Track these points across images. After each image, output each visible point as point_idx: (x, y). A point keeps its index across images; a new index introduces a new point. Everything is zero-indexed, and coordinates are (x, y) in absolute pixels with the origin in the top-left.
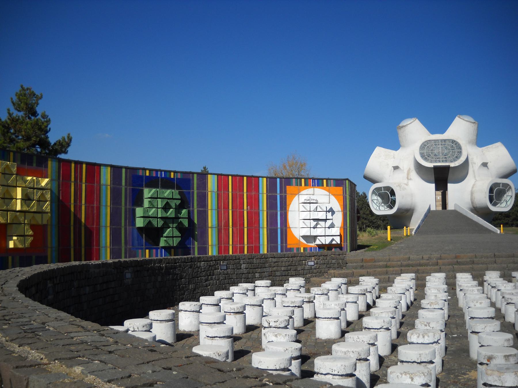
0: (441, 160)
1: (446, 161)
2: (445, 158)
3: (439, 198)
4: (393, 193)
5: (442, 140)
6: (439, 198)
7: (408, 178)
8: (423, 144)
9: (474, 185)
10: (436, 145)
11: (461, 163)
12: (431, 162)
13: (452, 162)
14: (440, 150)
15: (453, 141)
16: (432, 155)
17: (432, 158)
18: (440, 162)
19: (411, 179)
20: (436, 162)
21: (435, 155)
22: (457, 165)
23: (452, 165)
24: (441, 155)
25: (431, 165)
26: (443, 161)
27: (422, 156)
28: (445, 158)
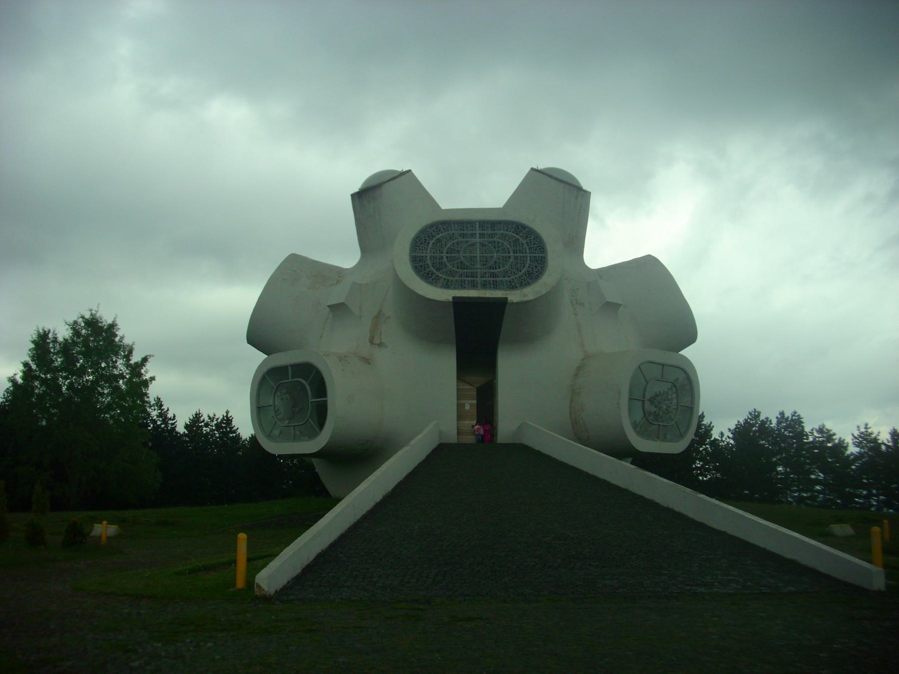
0: (479, 280)
1: (495, 286)
2: (493, 275)
3: (470, 405)
4: (320, 387)
5: (483, 224)
6: (467, 407)
7: (371, 342)
8: (423, 231)
9: (579, 369)
10: (463, 235)
11: (544, 292)
12: (447, 286)
13: (512, 287)
14: (478, 254)
15: (520, 228)
16: (450, 266)
17: (452, 273)
18: (474, 286)
19: (381, 345)
20: (462, 286)
21: (462, 266)
22: (531, 297)
23: (514, 296)
24: (478, 266)
25: (446, 295)
26: (484, 286)
27: (420, 266)
28: (493, 275)
